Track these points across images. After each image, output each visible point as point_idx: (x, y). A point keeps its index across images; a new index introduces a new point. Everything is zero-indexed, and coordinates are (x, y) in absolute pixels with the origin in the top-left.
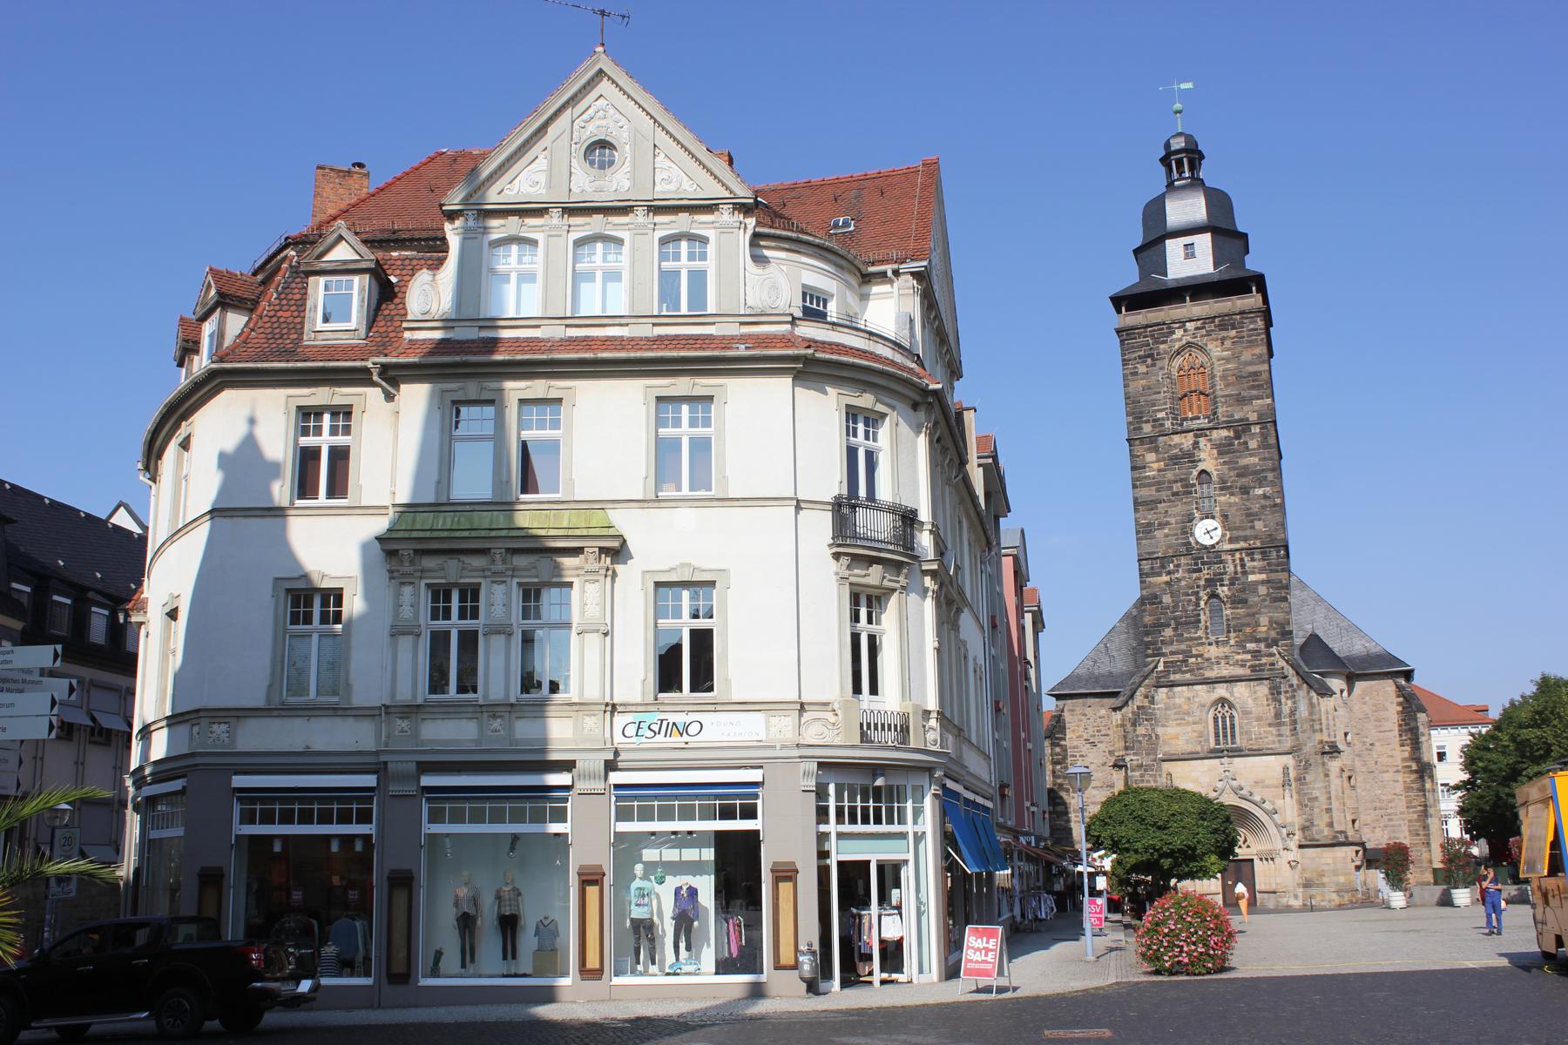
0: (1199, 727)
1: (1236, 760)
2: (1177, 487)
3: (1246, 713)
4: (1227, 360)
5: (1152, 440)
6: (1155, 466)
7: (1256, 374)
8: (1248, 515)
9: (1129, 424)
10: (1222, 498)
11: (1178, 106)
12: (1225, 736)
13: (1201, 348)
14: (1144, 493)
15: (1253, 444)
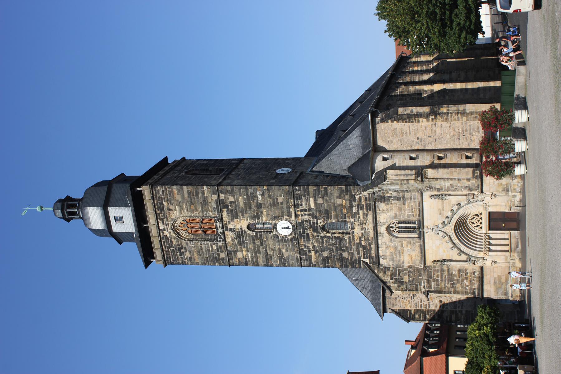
0: (405, 243)
1: (425, 224)
2: (258, 243)
3: (396, 216)
4: (181, 209)
5: (229, 253)
6: (245, 253)
7: (189, 193)
8: (274, 205)
9: (220, 264)
10: (264, 219)
11: (38, 209)
12: (410, 227)
13: (175, 221)
14: (261, 260)
15: (231, 199)
